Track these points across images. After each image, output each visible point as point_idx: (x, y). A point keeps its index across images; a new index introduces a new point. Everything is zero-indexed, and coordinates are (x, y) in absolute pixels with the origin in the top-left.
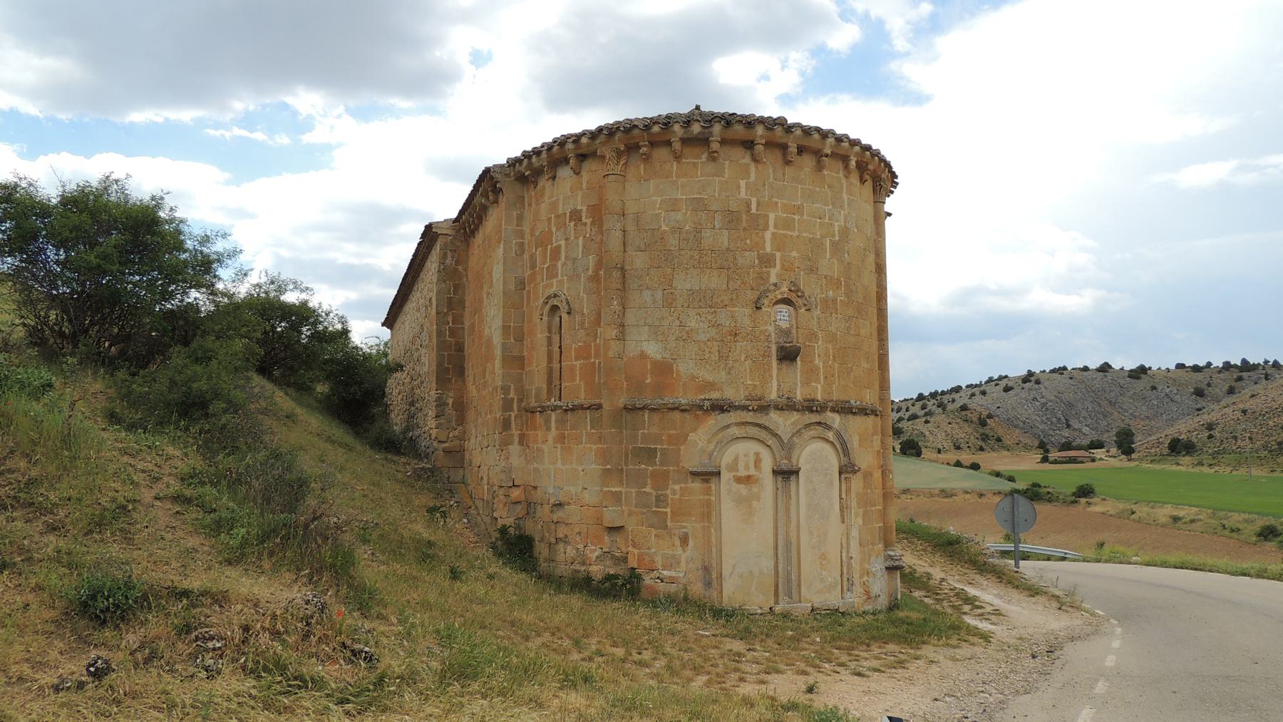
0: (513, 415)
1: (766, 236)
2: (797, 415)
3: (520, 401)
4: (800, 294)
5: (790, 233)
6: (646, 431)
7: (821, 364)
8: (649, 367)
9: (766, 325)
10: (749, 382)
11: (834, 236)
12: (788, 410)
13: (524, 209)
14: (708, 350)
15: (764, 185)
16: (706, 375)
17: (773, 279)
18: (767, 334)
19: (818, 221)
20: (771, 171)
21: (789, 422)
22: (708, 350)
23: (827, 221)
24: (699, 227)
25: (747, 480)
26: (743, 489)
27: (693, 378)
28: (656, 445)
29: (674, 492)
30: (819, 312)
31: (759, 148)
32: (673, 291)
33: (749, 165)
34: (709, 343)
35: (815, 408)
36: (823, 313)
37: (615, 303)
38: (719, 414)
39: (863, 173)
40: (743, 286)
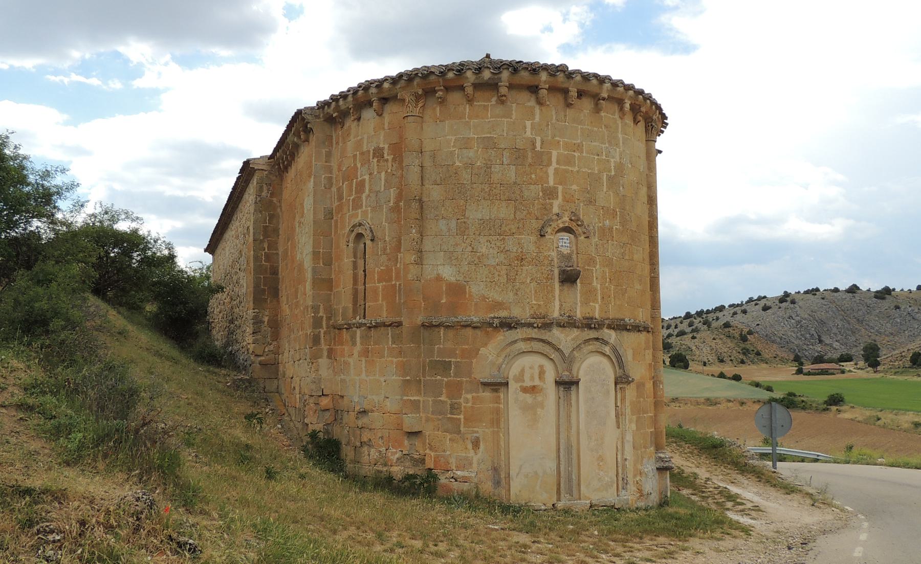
0: (322, 331)
1: (549, 171)
2: (577, 331)
3: (329, 319)
4: (580, 223)
5: (570, 169)
6: (441, 346)
7: (599, 286)
8: (444, 288)
9: (549, 251)
10: (534, 302)
11: (610, 171)
12: (569, 328)
13: (332, 146)
14: (497, 273)
15: (548, 125)
16: (495, 295)
17: (556, 210)
19: (596, 157)
20: (554, 113)
21: (569, 338)
22: (497, 273)
23: (604, 157)
24: (489, 163)
25: (533, 390)
26: (528, 398)
27: (484, 298)
28: (450, 358)
29: (467, 401)
31: (543, 93)
32: (465, 220)
33: (535, 107)
34: (498, 267)
35: (593, 326)
37: (414, 231)
38: (507, 330)
39: (636, 115)
40: (528, 216)
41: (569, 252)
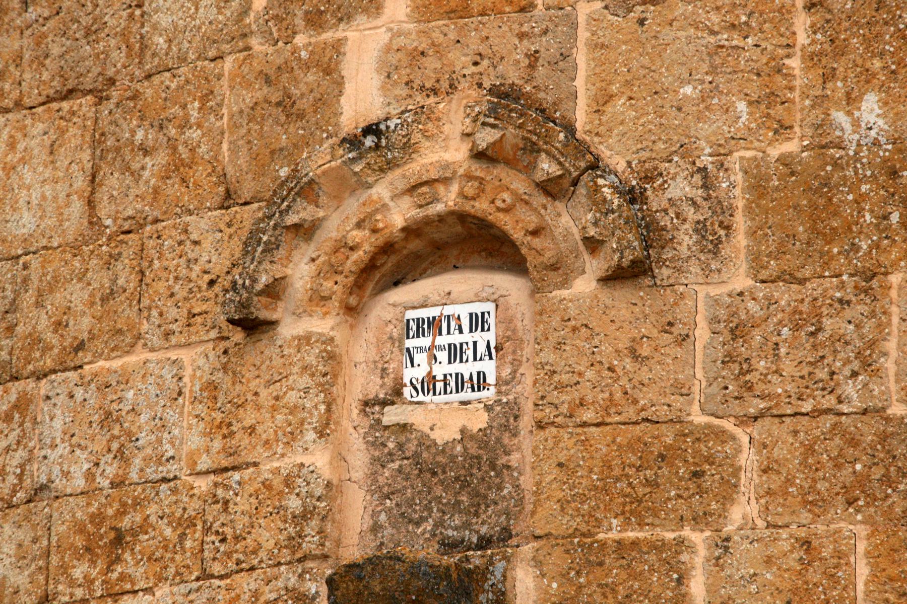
18: (294, 504)
30: (742, 281)
36: (791, 278)
40: (173, 188)
41: (478, 421)
